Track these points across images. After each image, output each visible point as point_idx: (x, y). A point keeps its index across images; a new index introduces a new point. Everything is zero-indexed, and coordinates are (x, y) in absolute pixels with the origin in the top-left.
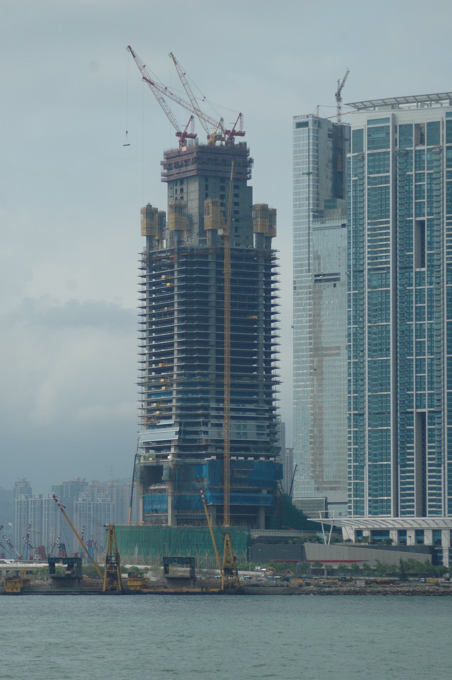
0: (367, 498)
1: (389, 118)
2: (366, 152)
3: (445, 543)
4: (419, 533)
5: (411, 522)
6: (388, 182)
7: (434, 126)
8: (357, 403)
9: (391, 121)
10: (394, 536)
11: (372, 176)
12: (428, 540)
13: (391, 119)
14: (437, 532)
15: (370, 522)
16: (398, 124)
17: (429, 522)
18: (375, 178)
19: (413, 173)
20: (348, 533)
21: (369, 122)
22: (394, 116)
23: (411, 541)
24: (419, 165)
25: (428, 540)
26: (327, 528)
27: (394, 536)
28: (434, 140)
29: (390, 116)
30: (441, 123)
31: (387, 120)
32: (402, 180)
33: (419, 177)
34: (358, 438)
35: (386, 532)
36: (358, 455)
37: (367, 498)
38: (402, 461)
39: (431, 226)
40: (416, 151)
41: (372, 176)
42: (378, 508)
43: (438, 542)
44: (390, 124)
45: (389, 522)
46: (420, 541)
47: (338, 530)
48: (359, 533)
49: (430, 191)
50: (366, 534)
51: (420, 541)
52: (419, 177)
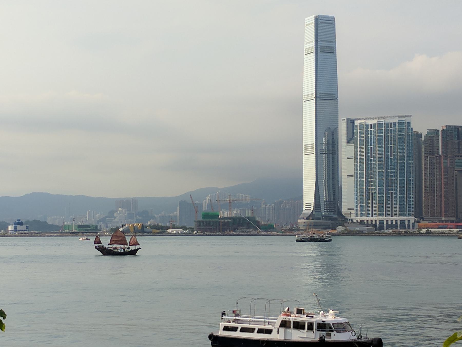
0: (359, 213)
2: (358, 130)
4: (372, 221)
5: (370, 218)
7: (375, 124)
8: (357, 190)
10: (365, 221)
12: (374, 223)
14: (376, 221)
15: (359, 218)
17: (374, 218)
20: (355, 221)
23: (370, 223)
24: (371, 134)
25: (374, 223)
26: (350, 220)
27: (365, 221)
28: (375, 127)
32: (367, 137)
34: (357, 198)
35: (364, 221)
36: (357, 202)
37: (359, 213)
38: (367, 204)
42: (361, 215)
43: (376, 223)
45: (364, 218)
46: (372, 223)
47: (352, 220)
48: (357, 221)
50: (359, 221)
51: (372, 223)
52: (371, 137)
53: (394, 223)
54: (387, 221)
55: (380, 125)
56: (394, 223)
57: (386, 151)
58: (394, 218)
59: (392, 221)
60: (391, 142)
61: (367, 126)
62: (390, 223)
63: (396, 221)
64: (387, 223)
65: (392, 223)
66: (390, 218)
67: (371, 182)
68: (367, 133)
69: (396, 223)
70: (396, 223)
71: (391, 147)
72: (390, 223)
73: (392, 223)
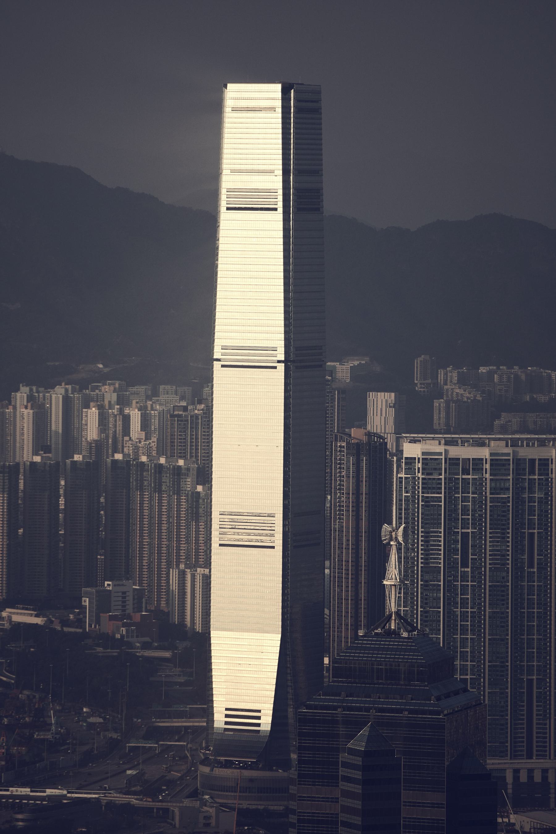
1: (510, 453)
3: (551, 778)
6: (441, 502)
9: (511, 456)
11: (425, 495)
13: (511, 454)
16: (449, 457)
18: (427, 497)
19: (460, 495)
21: (423, 454)
22: (445, 450)
29: (511, 452)
30: (550, 460)
31: (440, 454)
32: (450, 500)
33: (465, 499)
39: (474, 537)
40: (462, 478)
41: (425, 495)
44: (443, 457)
49: (474, 510)
53: (538, 778)
54: (516, 771)
55: (498, 464)
56: (538, 778)
57: (517, 548)
58: (536, 763)
59: (530, 771)
60: (531, 522)
61: (453, 462)
62: (523, 778)
63: (545, 771)
64: (516, 778)
65: (530, 777)
66: (524, 764)
67: (463, 646)
68: (452, 487)
69: (545, 778)
70: (545, 778)
71: (532, 535)
72: (523, 778)
73: (530, 777)
